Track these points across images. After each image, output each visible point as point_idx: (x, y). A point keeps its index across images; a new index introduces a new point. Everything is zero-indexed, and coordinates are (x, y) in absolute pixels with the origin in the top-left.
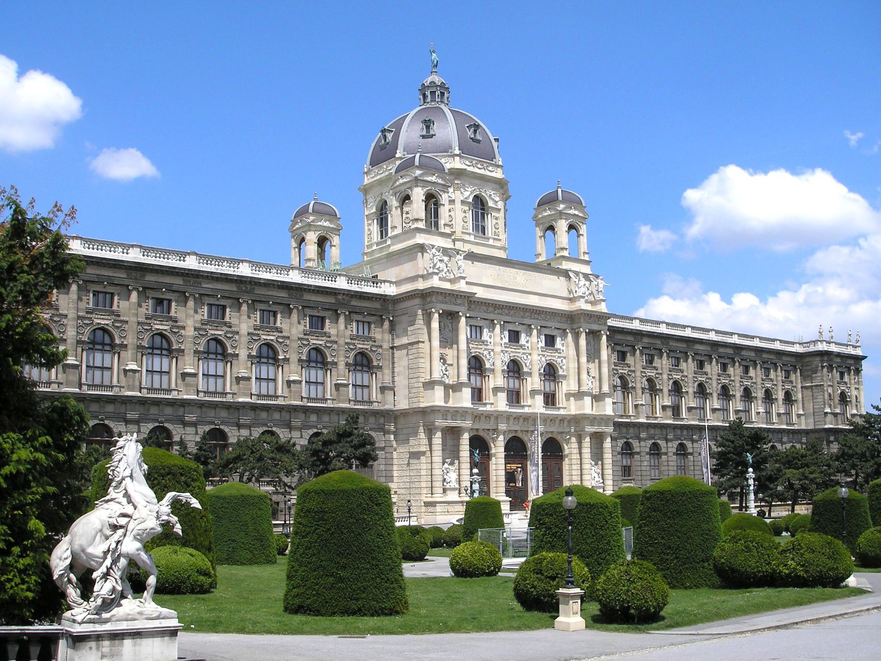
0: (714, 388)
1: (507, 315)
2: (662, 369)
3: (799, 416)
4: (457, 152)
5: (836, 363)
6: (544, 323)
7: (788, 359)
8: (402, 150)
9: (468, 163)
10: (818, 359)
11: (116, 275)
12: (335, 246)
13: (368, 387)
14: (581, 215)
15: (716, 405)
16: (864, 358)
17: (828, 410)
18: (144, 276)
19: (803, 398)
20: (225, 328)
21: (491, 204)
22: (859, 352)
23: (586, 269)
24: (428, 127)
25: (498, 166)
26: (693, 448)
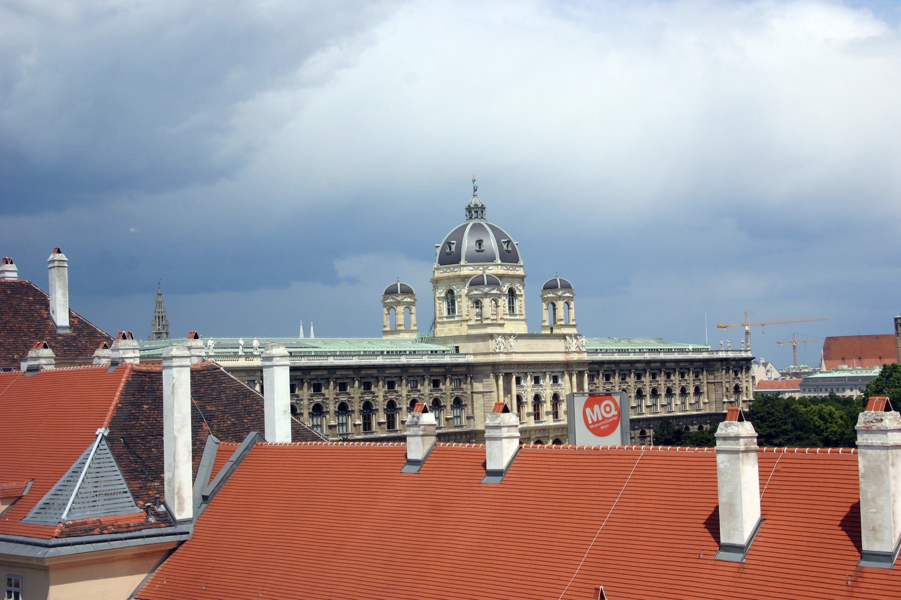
0: (647, 391)
1: (534, 368)
2: (615, 383)
3: (705, 403)
4: (499, 262)
5: (732, 365)
6: (552, 370)
7: (698, 364)
8: (464, 259)
9: (505, 268)
10: (719, 363)
11: (349, 373)
12: (413, 313)
13: (459, 417)
14: (571, 296)
15: (649, 404)
16: (753, 358)
17: (725, 400)
18: (360, 371)
19: (707, 390)
20: (395, 394)
21: (518, 293)
22: (749, 355)
23: (573, 331)
24: (480, 245)
25: (521, 266)
26: (635, 434)
